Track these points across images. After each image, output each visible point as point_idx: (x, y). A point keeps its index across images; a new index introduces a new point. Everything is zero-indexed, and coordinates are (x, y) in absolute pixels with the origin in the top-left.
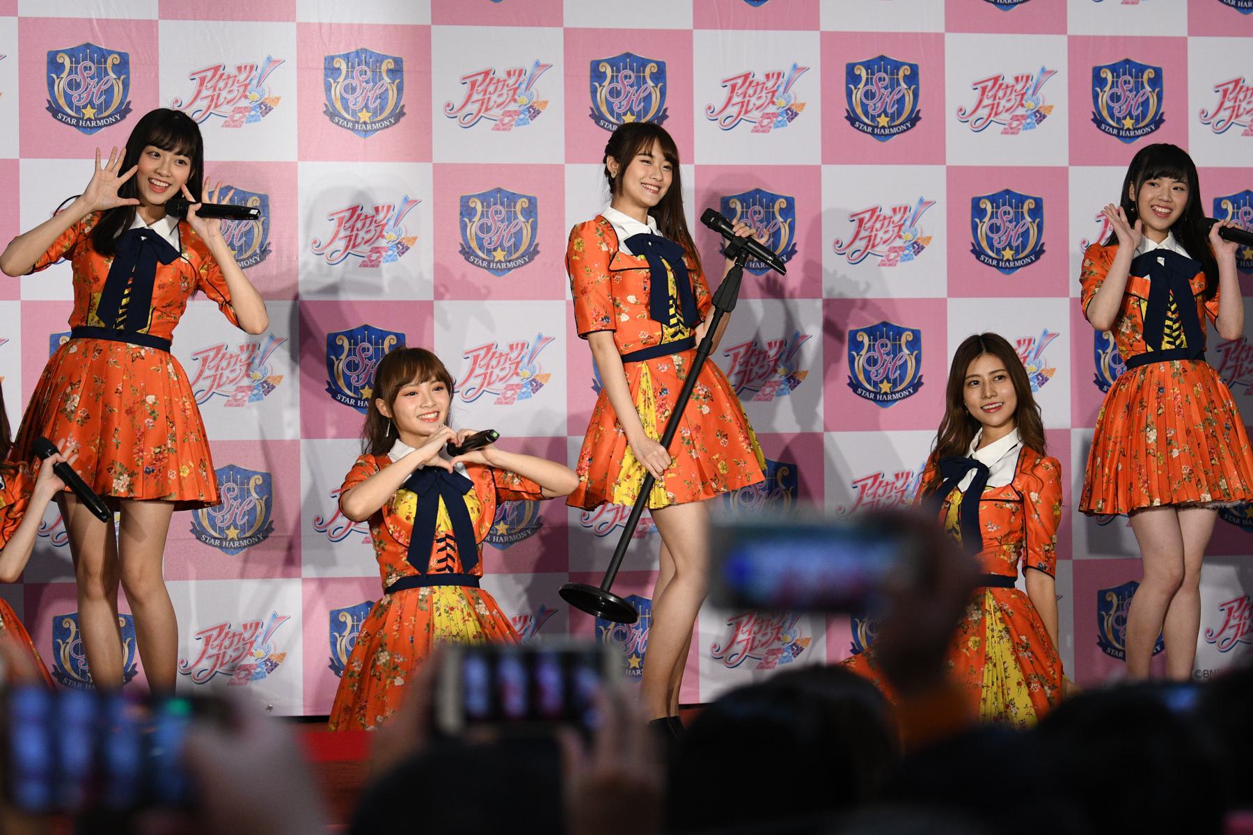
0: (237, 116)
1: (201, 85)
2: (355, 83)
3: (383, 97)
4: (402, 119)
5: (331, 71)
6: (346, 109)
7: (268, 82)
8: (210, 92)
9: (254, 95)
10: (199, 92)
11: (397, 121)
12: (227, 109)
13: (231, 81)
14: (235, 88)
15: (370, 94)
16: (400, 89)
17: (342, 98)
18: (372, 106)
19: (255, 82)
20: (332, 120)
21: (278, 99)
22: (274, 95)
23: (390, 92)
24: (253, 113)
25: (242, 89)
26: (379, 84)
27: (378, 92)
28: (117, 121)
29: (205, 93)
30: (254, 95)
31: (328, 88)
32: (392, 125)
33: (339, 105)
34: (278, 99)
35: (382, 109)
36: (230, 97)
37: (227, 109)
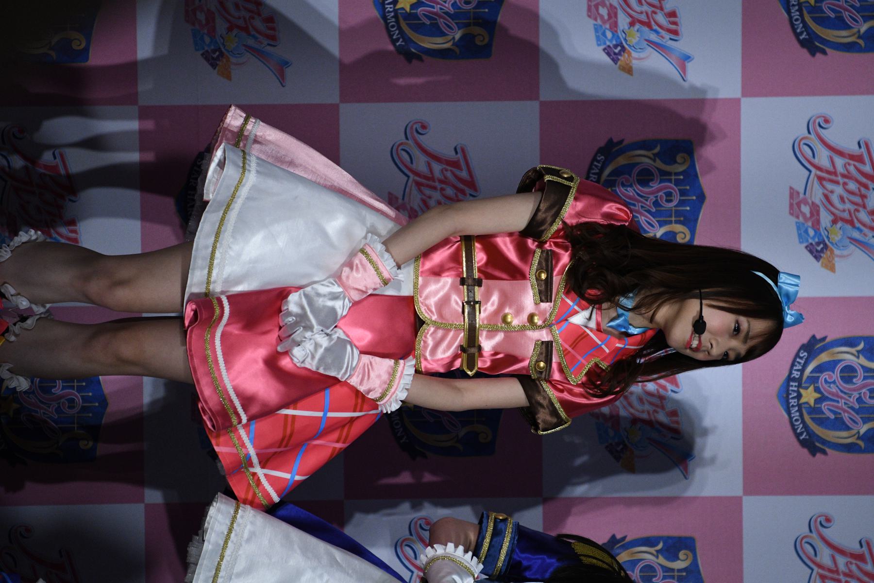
0: (806, 209)
1: (852, 157)
2: (858, 381)
3: (839, 424)
4: (805, 451)
5: (873, 347)
6: (820, 369)
7: (858, 254)
8: (840, 168)
9: (837, 234)
10: (841, 154)
11: (804, 443)
12: (817, 194)
13: (857, 199)
14: (848, 206)
15: (841, 403)
16: (849, 448)
17: (836, 363)
18: (824, 406)
19: (856, 235)
20: (804, 347)
21: (832, 269)
22: (839, 263)
23: (844, 434)
24: (811, 232)
25: (846, 215)
26: (858, 418)
27: (846, 416)
28: (797, 35)
29: (840, 162)
30: (837, 234)
31: (850, 342)
32: (798, 436)
33: (824, 357)
34: (832, 269)
35: (822, 422)
36: (835, 199)
37: (817, 194)
